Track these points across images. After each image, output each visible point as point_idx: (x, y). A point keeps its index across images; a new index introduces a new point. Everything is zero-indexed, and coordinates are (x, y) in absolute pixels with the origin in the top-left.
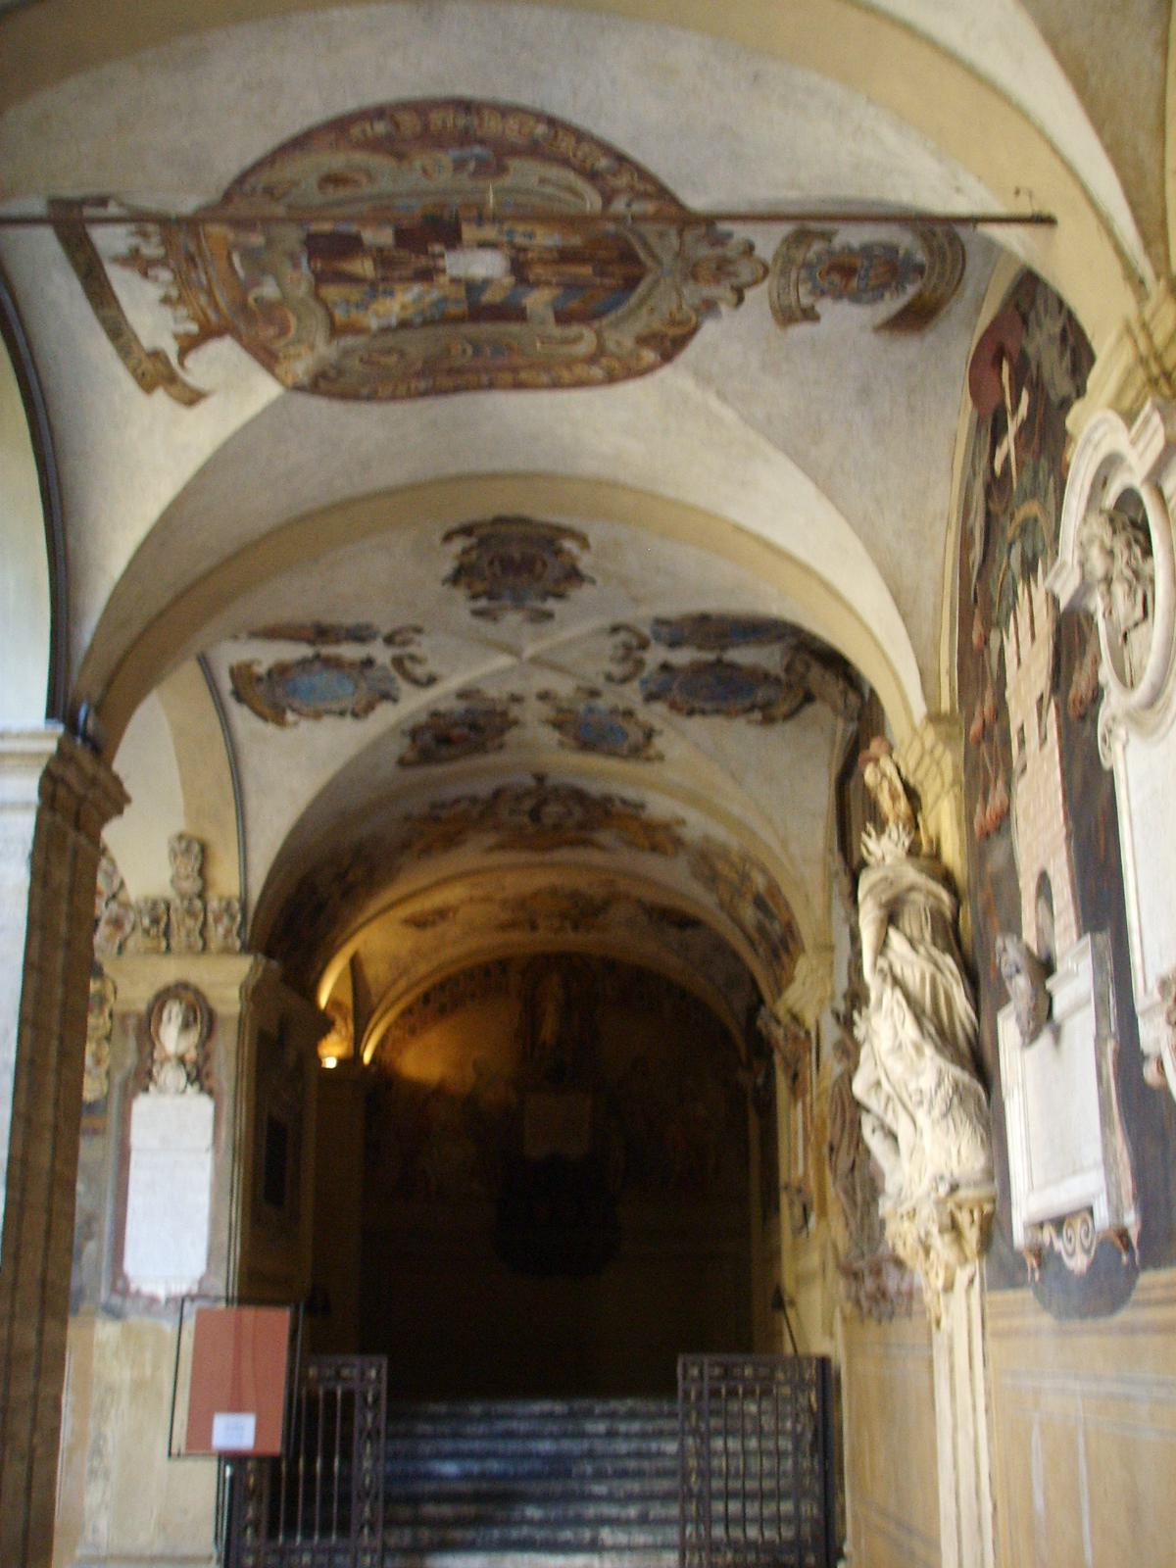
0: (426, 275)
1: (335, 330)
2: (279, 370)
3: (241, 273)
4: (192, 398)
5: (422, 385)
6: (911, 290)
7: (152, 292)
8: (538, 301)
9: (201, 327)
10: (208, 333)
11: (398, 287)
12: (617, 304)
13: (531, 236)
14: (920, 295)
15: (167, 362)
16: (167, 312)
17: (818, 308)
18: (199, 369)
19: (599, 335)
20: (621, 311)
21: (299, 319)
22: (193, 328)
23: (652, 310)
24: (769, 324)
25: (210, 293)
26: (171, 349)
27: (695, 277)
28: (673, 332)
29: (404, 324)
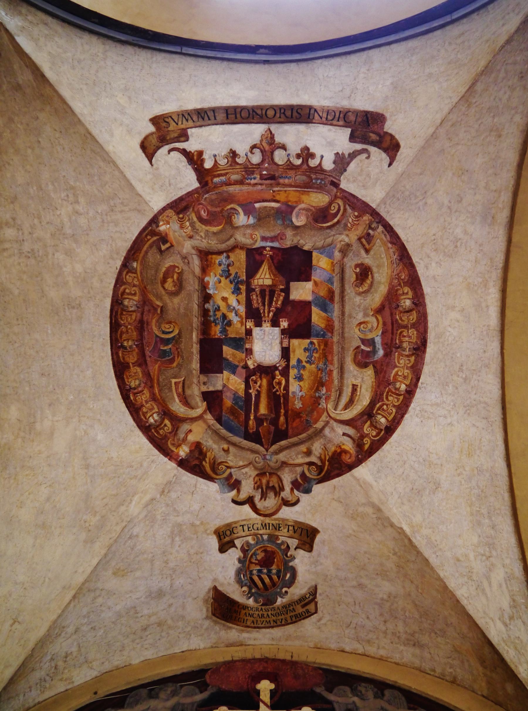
0: (254, 315)
1: (205, 255)
2: (170, 212)
3: (257, 205)
4: (148, 149)
5: (131, 303)
6: (251, 602)
7: (242, 149)
8: (232, 382)
9: (208, 171)
10: (202, 174)
11: (243, 297)
12: (230, 429)
13: (300, 378)
14: (245, 607)
15: (177, 140)
16: (224, 152)
17: (232, 551)
18: (169, 160)
19: (200, 417)
20: (224, 432)
21: (214, 233)
22: (208, 165)
23: (227, 451)
24: (218, 523)
25: (236, 183)
26: (192, 146)
27: (261, 474)
28: (207, 466)
29: (207, 298)
